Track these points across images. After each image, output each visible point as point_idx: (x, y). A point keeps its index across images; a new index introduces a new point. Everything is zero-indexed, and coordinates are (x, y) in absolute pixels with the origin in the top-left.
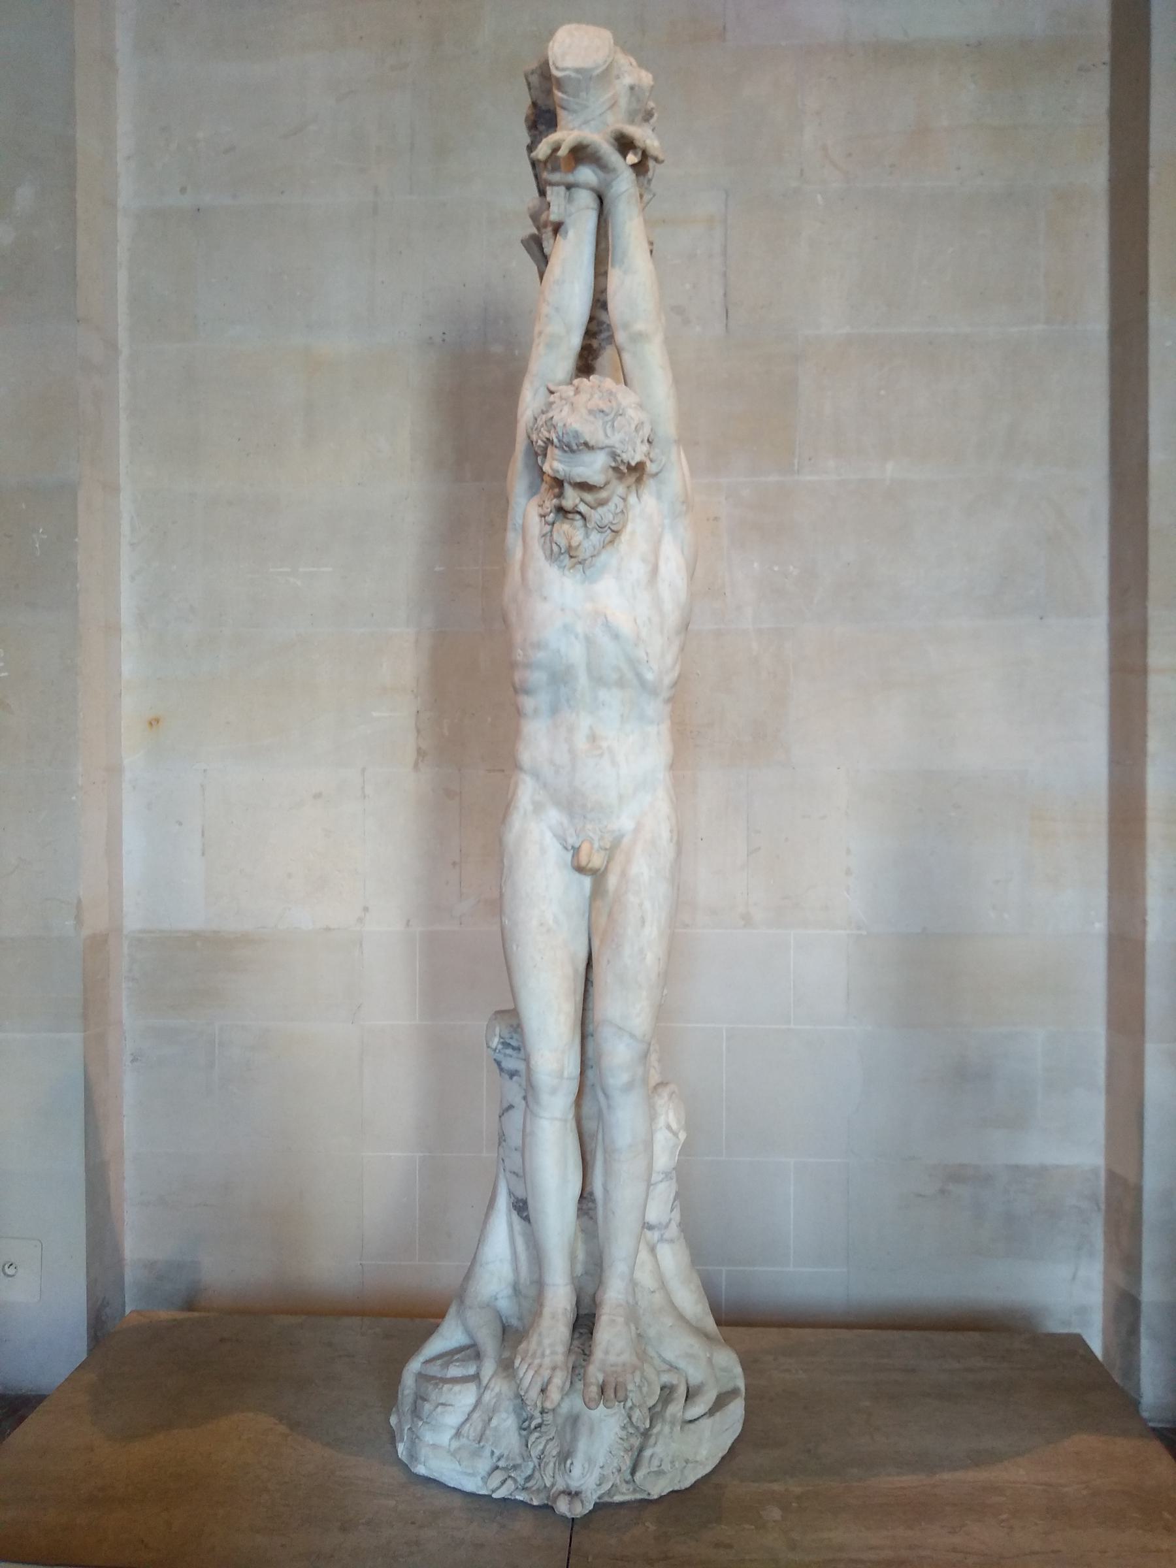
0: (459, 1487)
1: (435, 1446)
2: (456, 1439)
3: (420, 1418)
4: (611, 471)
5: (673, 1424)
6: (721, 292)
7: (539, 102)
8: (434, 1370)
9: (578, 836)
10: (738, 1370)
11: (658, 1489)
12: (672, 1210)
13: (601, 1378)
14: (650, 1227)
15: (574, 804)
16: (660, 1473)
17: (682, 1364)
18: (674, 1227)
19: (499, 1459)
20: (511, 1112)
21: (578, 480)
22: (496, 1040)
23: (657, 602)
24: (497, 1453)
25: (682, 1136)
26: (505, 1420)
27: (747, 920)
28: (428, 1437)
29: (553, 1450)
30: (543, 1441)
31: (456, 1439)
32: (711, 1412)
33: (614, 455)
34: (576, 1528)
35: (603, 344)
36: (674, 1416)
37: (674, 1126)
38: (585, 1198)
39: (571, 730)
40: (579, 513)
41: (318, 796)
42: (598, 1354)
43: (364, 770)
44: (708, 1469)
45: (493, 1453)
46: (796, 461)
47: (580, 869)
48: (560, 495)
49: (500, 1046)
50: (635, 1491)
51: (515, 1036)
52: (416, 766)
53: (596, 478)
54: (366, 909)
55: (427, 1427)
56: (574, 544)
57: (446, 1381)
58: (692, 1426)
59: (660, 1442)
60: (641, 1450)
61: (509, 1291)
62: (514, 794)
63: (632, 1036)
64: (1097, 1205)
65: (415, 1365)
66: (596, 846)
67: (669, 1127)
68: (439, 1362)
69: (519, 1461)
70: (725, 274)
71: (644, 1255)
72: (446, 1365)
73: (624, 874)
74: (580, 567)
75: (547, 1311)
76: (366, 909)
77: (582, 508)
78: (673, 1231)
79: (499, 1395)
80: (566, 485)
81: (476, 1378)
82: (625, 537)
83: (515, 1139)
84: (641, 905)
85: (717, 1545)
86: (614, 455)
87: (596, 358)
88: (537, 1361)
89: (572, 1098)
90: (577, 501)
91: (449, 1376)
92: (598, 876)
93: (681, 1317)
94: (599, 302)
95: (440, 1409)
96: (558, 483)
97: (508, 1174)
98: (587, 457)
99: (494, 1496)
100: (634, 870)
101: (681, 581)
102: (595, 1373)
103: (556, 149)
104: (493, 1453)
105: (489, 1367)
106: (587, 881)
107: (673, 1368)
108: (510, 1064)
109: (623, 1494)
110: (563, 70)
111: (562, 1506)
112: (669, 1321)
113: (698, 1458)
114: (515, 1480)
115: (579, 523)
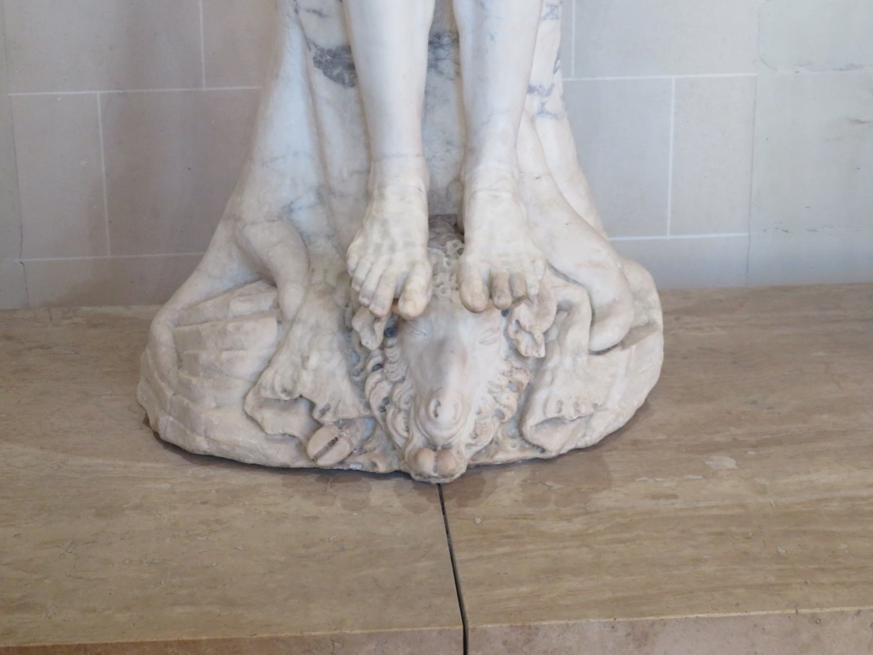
5: (576, 354)
11: (556, 442)
12: (555, 71)
14: (531, 90)
16: (557, 421)
17: (583, 275)
18: (557, 93)
26: (328, 361)
29: (402, 394)
32: (622, 344)
34: (446, 492)
59: (558, 381)
61: (311, 198)
71: (524, 127)
78: (554, 103)
85: (655, 497)
111: (428, 464)
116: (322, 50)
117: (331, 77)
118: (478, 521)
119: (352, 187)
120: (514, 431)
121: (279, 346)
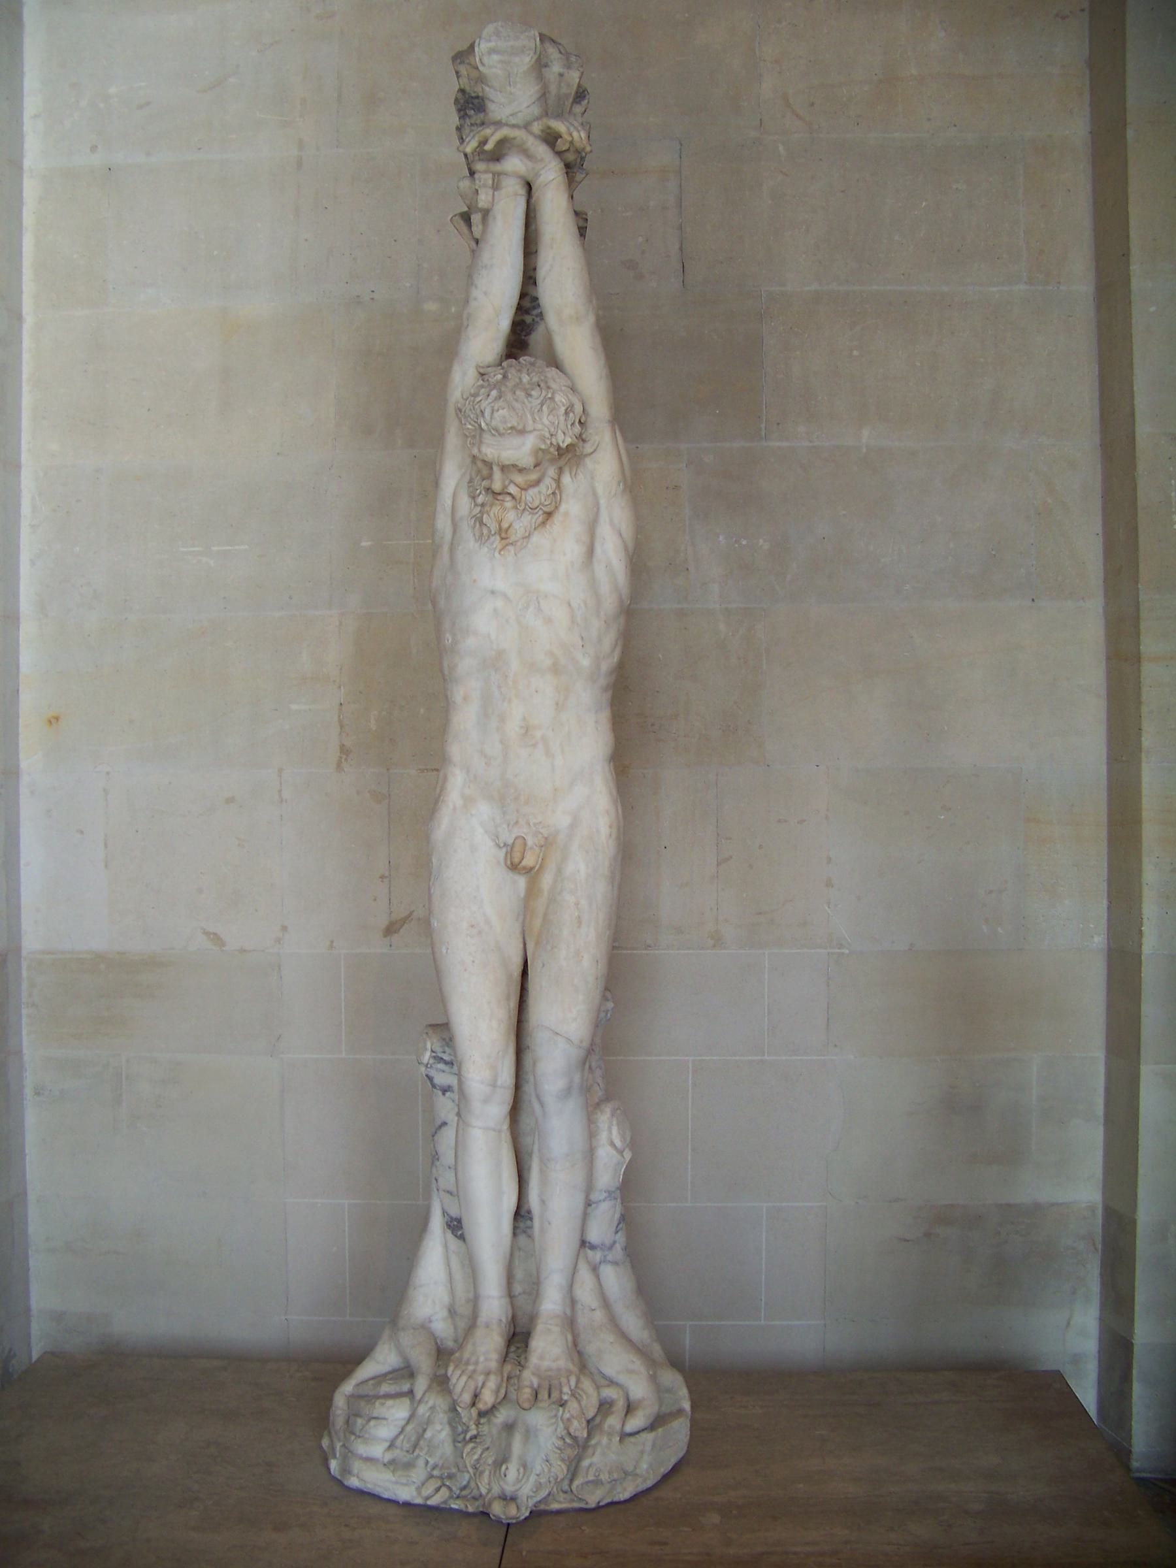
0: (394, 1498)
1: (369, 1460)
2: (389, 1451)
3: (354, 1434)
5: (610, 1434)
9: (510, 831)
10: (684, 1392)
11: (593, 1498)
12: (617, 1232)
13: (535, 1382)
14: (593, 1247)
15: (505, 796)
17: (622, 1379)
19: (434, 1468)
20: (444, 1129)
22: (428, 1054)
23: (593, 584)
24: (431, 1461)
25: (628, 1155)
26: (440, 1432)
27: (718, 940)
30: (479, 1451)
31: (389, 1451)
32: (652, 1427)
35: (538, 319)
36: (610, 1426)
37: (618, 1143)
38: (521, 1214)
39: (502, 719)
40: (509, 494)
41: (230, 800)
42: (534, 1359)
43: (281, 770)
44: (649, 1483)
45: (427, 1463)
46: (763, 426)
47: (514, 867)
48: (490, 477)
49: (432, 1061)
50: (572, 1501)
51: (447, 1049)
52: (339, 765)
53: (527, 461)
54: (285, 929)
55: (359, 1440)
56: (505, 525)
57: (377, 1397)
58: (632, 1439)
60: (579, 1459)
61: (445, 1313)
62: (443, 788)
63: (568, 1040)
64: (1094, 1244)
65: (348, 1387)
66: (530, 842)
67: (612, 1144)
68: (371, 1382)
69: (454, 1470)
71: (584, 1274)
72: (379, 1384)
73: (559, 871)
74: (511, 548)
75: (482, 1320)
76: (285, 929)
77: (512, 489)
79: (432, 1408)
80: (495, 468)
81: (411, 1393)
82: (557, 518)
83: (448, 1157)
84: (577, 904)
87: (529, 334)
88: (471, 1368)
89: (506, 1108)
92: (532, 874)
93: (623, 1336)
95: (372, 1423)
96: (489, 465)
97: (442, 1193)
98: (515, 441)
99: (429, 1503)
100: (570, 868)
102: (529, 1377)
104: (427, 1463)
106: (522, 882)
107: (612, 1383)
108: (441, 1079)
109: (560, 1502)
111: (497, 1509)
112: (608, 1337)
113: (638, 1471)
114: (449, 1488)
115: (509, 503)
118: (524, 1553)
120: (566, 1487)
121: (409, 1420)
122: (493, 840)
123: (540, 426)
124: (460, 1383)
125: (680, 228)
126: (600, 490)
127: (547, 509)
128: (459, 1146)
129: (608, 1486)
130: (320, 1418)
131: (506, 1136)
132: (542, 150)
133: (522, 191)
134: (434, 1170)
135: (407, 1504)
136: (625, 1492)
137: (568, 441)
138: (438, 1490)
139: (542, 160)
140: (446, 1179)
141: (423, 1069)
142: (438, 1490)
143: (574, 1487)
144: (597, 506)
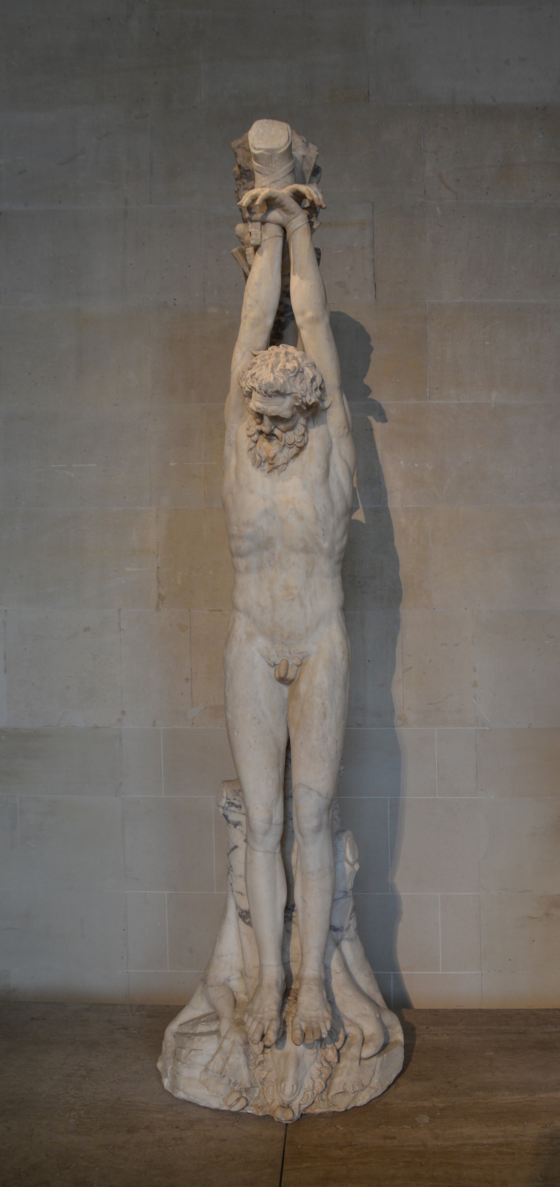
0: (208, 1106)
2: (203, 1073)
4: (295, 409)
6: (371, 273)
7: (243, 165)
8: (186, 1029)
19: (235, 1085)
20: (237, 851)
21: (274, 414)
22: (224, 801)
25: (357, 867)
28: (185, 1072)
33: (296, 398)
34: (289, 1129)
35: (289, 320)
38: (289, 908)
42: (302, 1010)
44: (379, 1093)
46: (428, 390)
49: (227, 805)
51: (237, 798)
61: (238, 975)
65: (173, 1027)
68: (191, 1023)
70: (373, 260)
74: (276, 471)
81: (217, 1032)
83: (239, 868)
85: (385, 1138)
86: (296, 398)
87: (283, 329)
89: (278, 838)
90: (273, 427)
91: (198, 1032)
94: (285, 293)
95: (193, 1053)
97: (235, 893)
98: (279, 400)
101: (344, 479)
103: (254, 199)
105: (225, 1025)
108: (234, 817)
109: (320, 1108)
110: (259, 149)
116: (242, 910)
117: (245, 923)
118: (299, 1146)
119: (254, 973)
122: (266, 662)
123: (295, 391)
124: (253, 1027)
125: (373, 260)
126: (332, 431)
127: (299, 445)
128: (248, 863)
129: (353, 1095)
130: (155, 1045)
131: (278, 856)
132: (292, 205)
133: (280, 234)
134: (230, 877)
135: (217, 1111)
136: (363, 1099)
137: (313, 400)
138: (238, 1100)
139: (293, 213)
140: (239, 885)
141: (221, 810)
142: (238, 1100)
143: (330, 1096)
144: (331, 442)
